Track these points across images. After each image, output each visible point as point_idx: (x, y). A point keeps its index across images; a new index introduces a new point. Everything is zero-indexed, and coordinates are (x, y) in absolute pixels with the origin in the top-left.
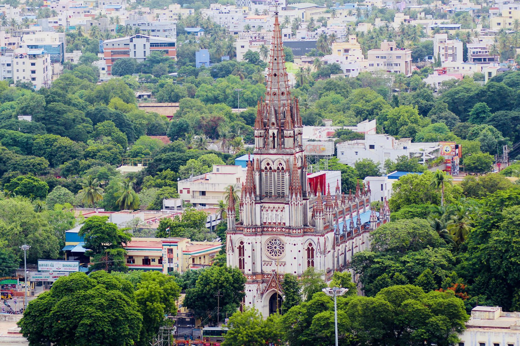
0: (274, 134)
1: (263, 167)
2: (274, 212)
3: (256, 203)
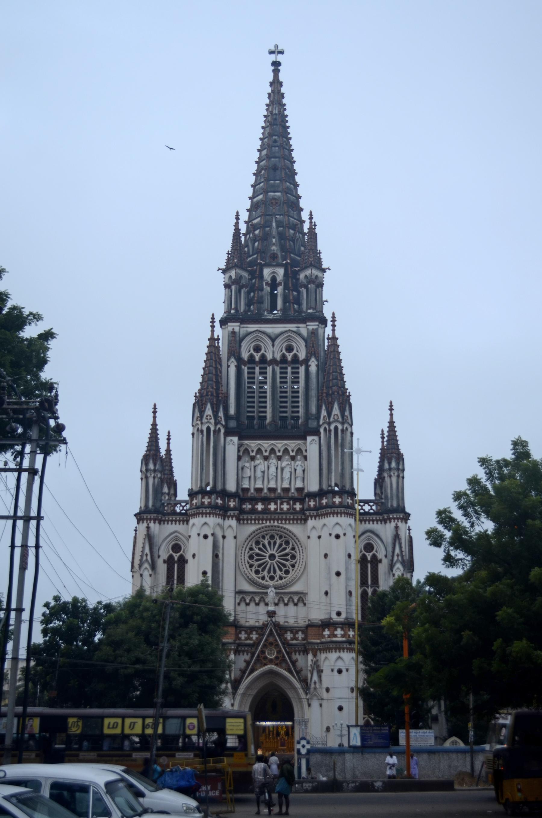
0: (274, 279)
1: (245, 356)
2: (273, 461)
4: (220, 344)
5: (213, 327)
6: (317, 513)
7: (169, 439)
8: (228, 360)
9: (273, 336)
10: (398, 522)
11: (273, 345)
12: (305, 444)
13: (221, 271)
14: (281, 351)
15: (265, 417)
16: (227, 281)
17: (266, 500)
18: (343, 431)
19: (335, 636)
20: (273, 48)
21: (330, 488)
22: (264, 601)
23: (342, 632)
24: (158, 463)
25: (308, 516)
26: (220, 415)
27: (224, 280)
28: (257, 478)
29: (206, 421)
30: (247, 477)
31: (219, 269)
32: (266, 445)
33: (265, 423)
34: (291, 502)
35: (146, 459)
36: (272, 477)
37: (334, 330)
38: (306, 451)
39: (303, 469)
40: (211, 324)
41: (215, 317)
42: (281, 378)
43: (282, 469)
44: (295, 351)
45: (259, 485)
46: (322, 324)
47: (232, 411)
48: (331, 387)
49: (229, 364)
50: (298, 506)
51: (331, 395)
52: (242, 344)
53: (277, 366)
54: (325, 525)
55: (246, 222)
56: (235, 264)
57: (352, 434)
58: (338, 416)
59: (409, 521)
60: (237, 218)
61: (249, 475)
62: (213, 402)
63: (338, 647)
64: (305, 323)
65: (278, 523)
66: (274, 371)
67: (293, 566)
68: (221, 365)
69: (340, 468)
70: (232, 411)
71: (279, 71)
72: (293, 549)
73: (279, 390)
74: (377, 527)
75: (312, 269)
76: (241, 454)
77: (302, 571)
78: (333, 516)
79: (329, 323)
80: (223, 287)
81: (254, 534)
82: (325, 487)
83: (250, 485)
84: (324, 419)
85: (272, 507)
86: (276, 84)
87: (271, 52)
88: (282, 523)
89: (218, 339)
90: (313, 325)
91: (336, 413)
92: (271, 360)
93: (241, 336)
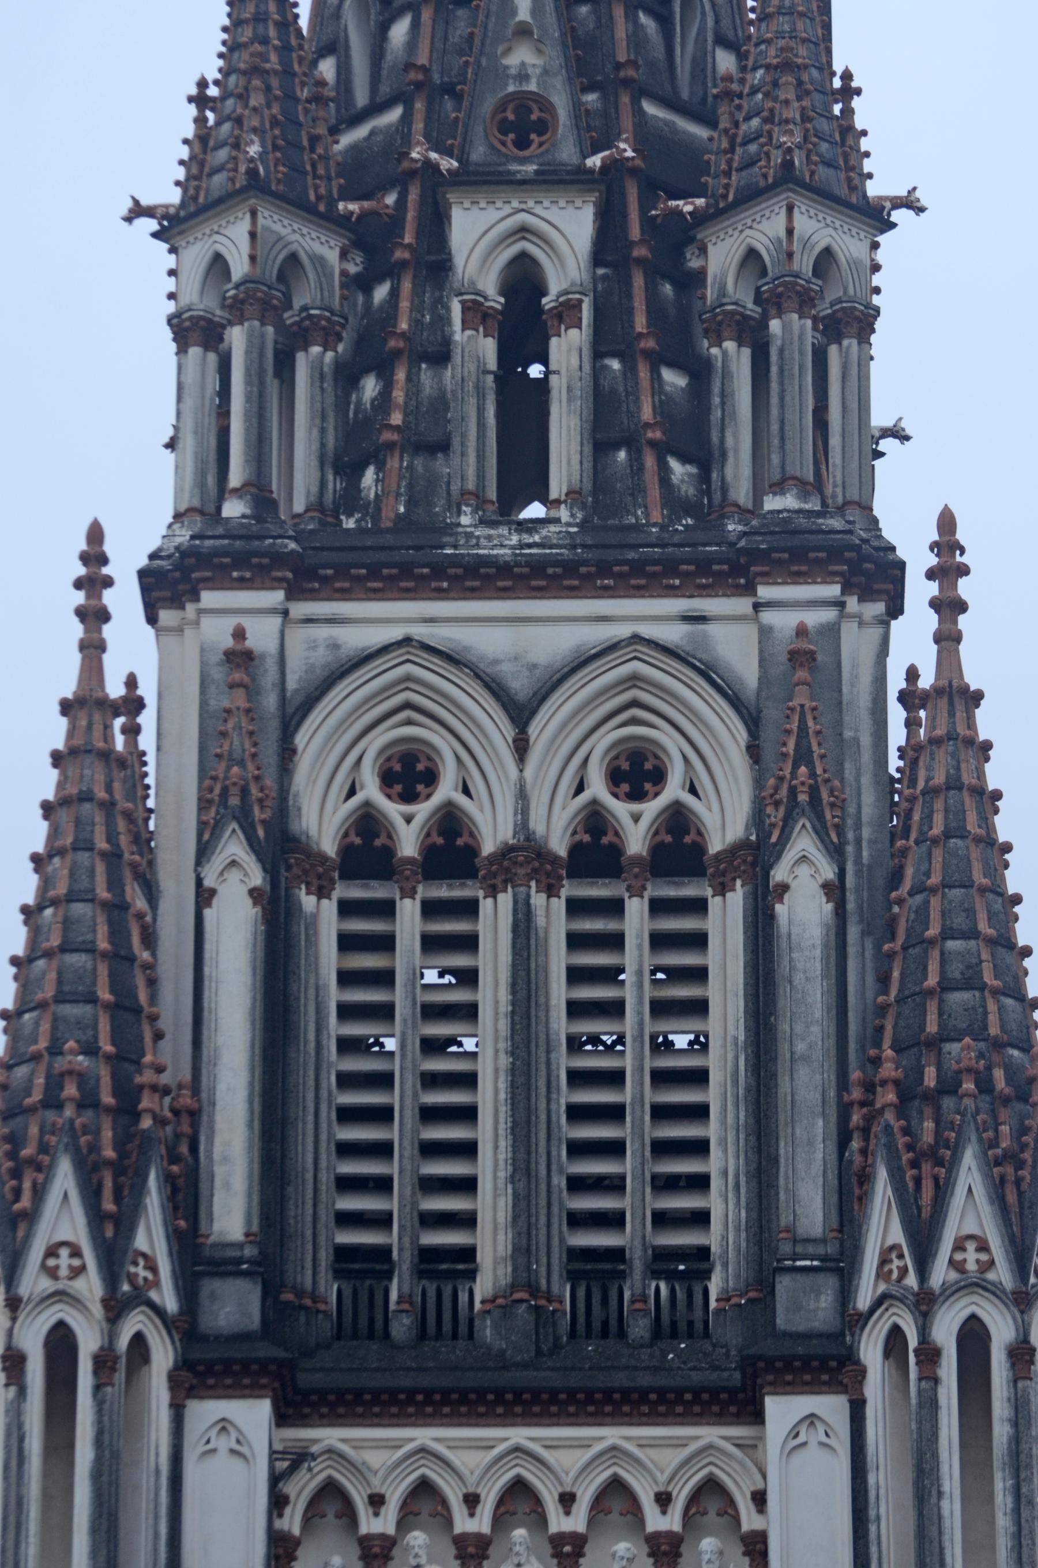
4: (147, 741)
8: (203, 852)
9: (520, 685)
11: (521, 748)
12: (751, 1448)
13: (152, 225)
14: (580, 789)
15: (468, 1254)
16: (190, 295)
26: (141, 1242)
27: (171, 284)
29: (46, 1285)
31: (138, 211)
32: (470, 1462)
33: (463, 1297)
38: (760, 1499)
40: (79, 598)
41: (109, 547)
42: (576, 975)
44: (673, 790)
46: (866, 596)
48: (935, 1043)
51: (933, 1097)
52: (300, 739)
56: (252, 173)
58: (983, 1247)
62: (94, 1147)
64: (749, 589)
68: (151, 892)
73: (563, 1062)
75: (790, 209)
76: (292, 1521)
80: (168, 334)
84: (882, 1274)
89: (133, 704)
91: (971, 1227)
92: (506, 852)
93: (291, 684)
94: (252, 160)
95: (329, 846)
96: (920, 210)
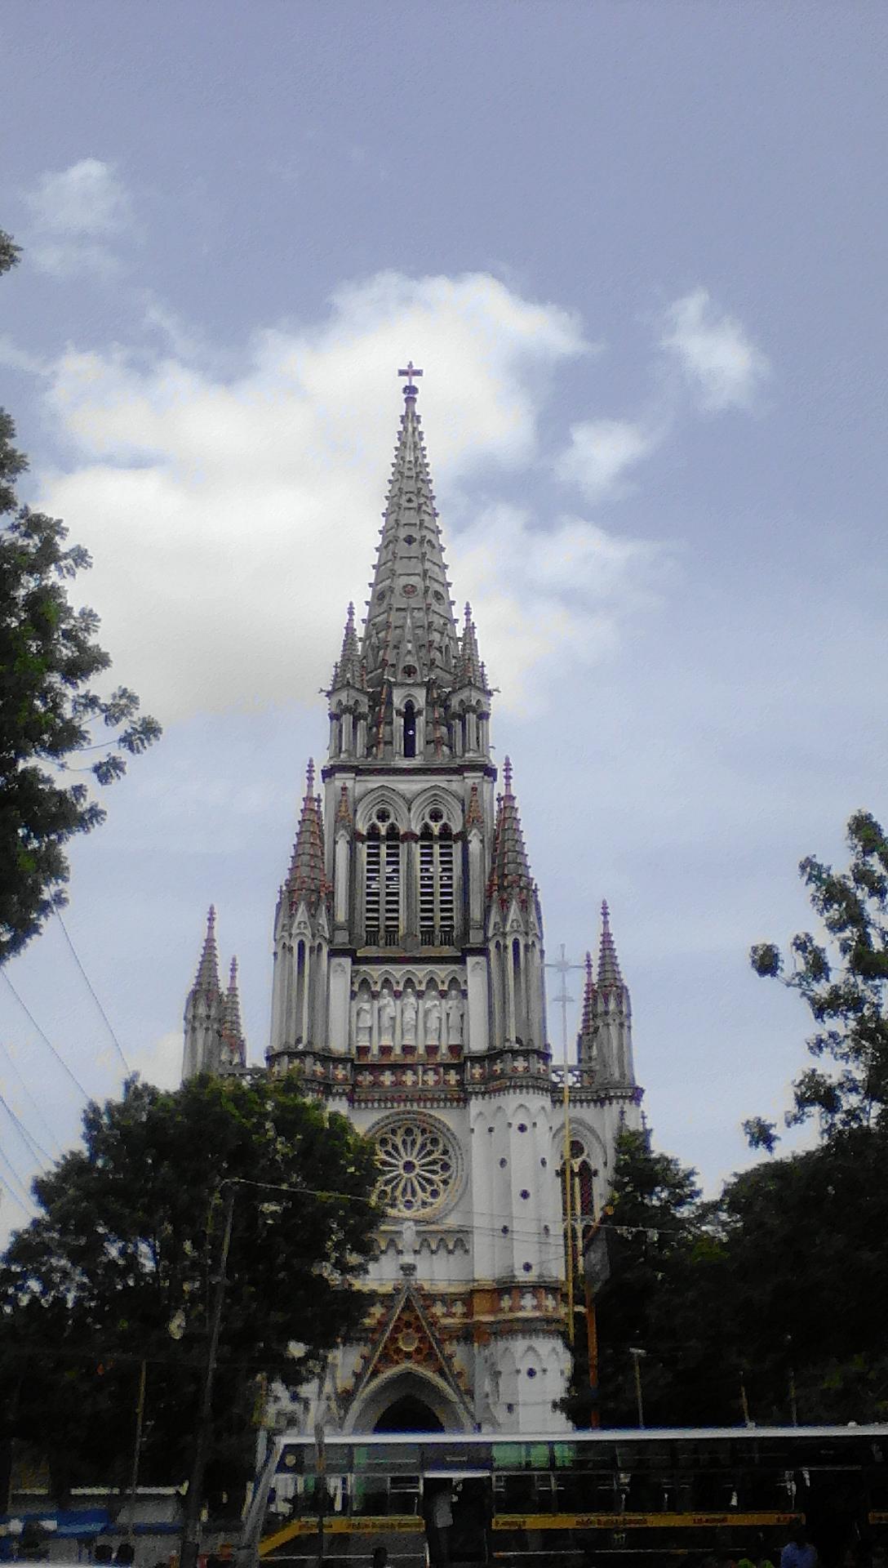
0: (409, 706)
3: (333, 953)
5: (310, 779)
6: (486, 1088)
7: (233, 970)
8: (336, 832)
9: (409, 796)
10: (624, 1103)
12: (464, 970)
13: (325, 694)
14: (423, 819)
15: (397, 926)
17: (398, 1068)
18: (527, 947)
19: (522, 1308)
20: (405, 368)
21: (507, 1044)
22: (395, 1246)
23: (535, 1302)
24: (214, 1004)
25: (471, 1093)
27: (329, 707)
28: (383, 1029)
29: (298, 931)
30: (365, 1028)
32: (398, 975)
33: (396, 937)
34: (442, 1070)
35: (194, 997)
36: (409, 1027)
37: (508, 785)
38: (466, 982)
39: (461, 1013)
43: (427, 1013)
44: (444, 820)
45: (386, 1041)
46: (489, 776)
47: (341, 916)
48: (506, 876)
49: (337, 839)
50: (453, 1077)
51: (505, 888)
53: (416, 842)
54: (500, 1108)
55: (364, 621)
56: (348, 682)
57: (542, 952)
59: (642, 1103)
60: (351, 613)
61: (369, 1025)
63: (528, 1328)
64: (462, 774)
65: (418, 1105)
66: (409, 853)
67: (445, 1182)
69: (524, 1011)
70: (341, 916)
71: (414, 400)
72: (445, 1152)
74: (587, 1113)
76: (356, 988)
77: (460, 1190)
78: (514, 1093)
79: (500, 774)
80: (328, 718)
81: (377, 1127)
82: (498, 1043)
83: (370, 1041)
84: (494, 928)
85: (409, 1078)
86: (410, 418)
87: (402, 373)
88: (425, 1107)
89: (319, 800)
90: (472, 778)
93: (356, 794)
94: (348, 679)
95: (365, 833)
96: (499, 692)
